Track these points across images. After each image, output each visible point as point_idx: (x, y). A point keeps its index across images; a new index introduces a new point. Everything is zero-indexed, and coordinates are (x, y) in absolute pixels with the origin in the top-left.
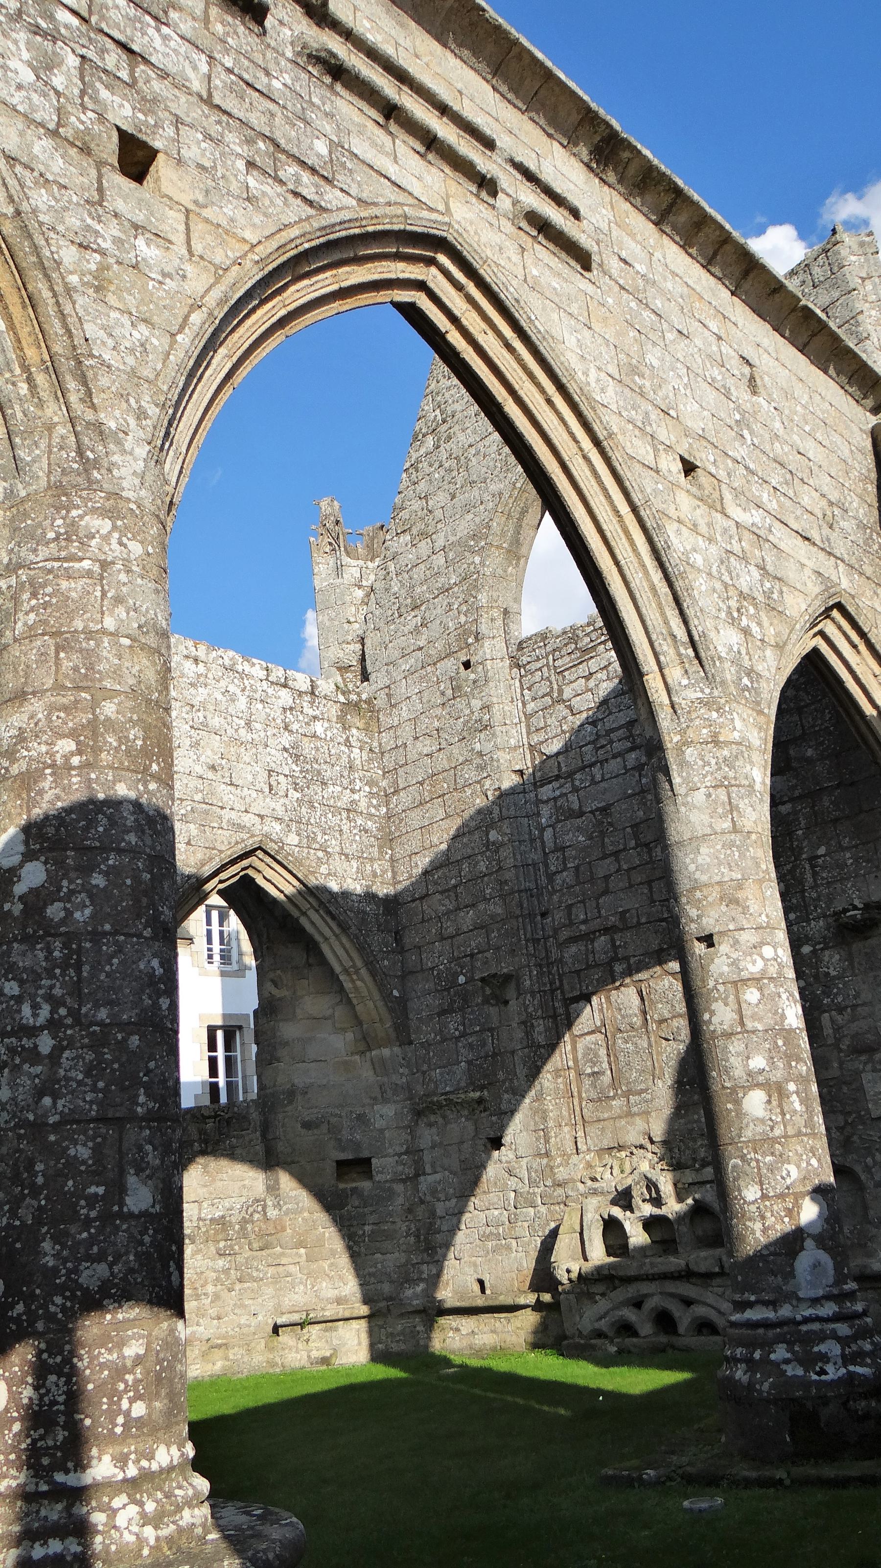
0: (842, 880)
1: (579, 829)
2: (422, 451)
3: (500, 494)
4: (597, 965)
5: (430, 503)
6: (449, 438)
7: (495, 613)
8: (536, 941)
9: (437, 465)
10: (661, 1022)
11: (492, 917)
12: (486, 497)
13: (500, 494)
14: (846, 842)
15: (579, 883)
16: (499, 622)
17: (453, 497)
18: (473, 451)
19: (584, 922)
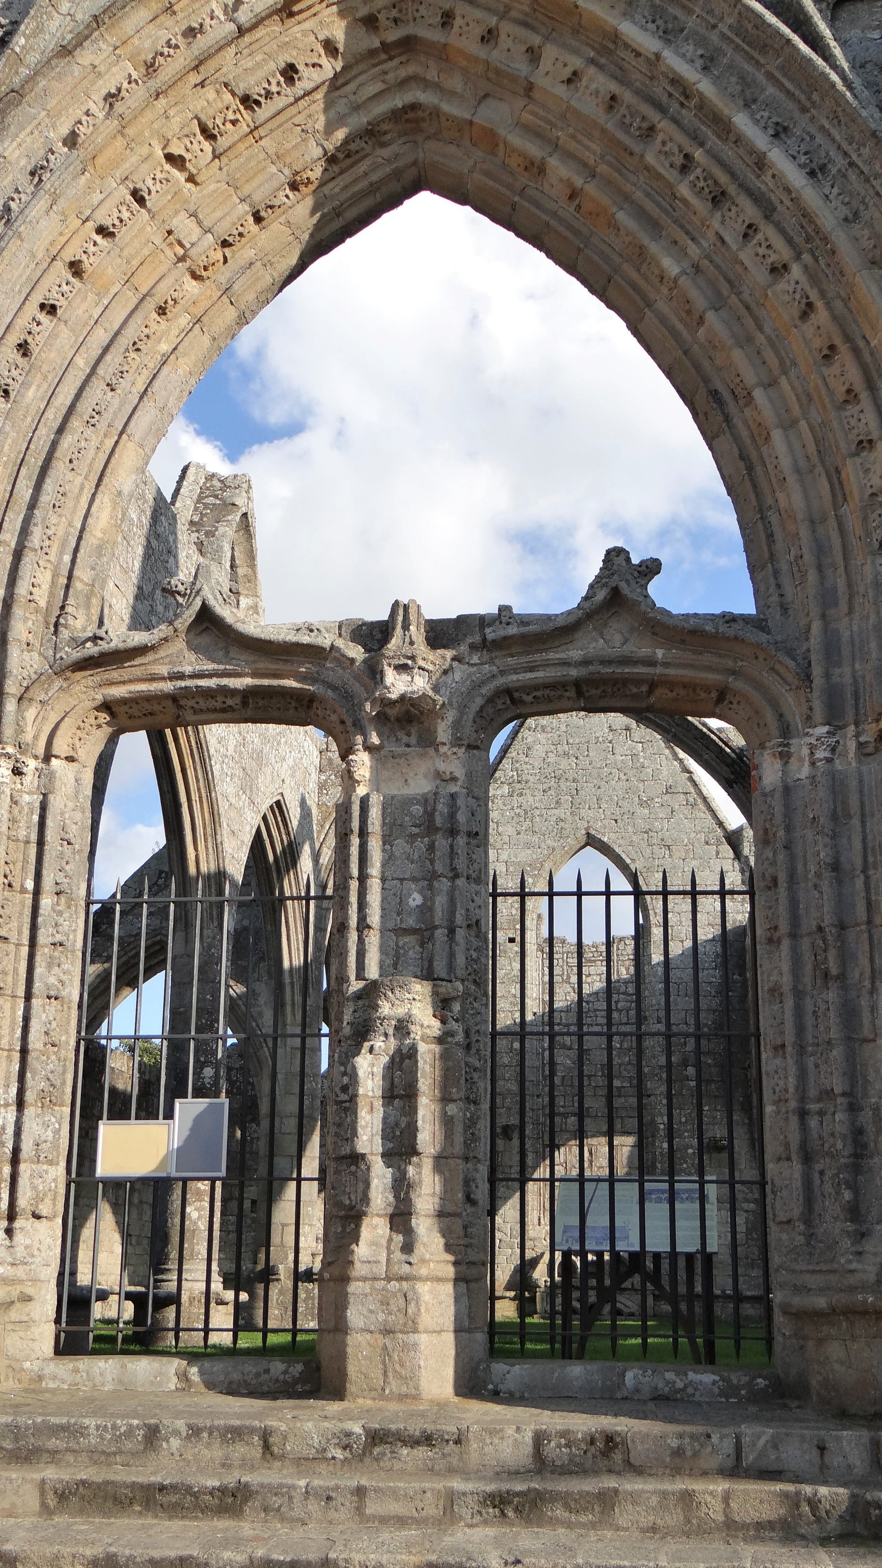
0: (714, 1124)
1: (568, 1056)
2: (499, 792)
3: (554, 849)
4: (567, 1131)
5: (500, 829)
6: (521, 795)
7: (535, 917)
8: (533, 1110)
9: (509, 807)
10: (599, 1168)
11: (508, 1090)
12: (543, 845)
13: (554, 849)
14: (719, 1107)
15: (562, 1085)
16: (535, 922)
17: (518, 833)
18: (537, 812)
19: (563, 1107)
